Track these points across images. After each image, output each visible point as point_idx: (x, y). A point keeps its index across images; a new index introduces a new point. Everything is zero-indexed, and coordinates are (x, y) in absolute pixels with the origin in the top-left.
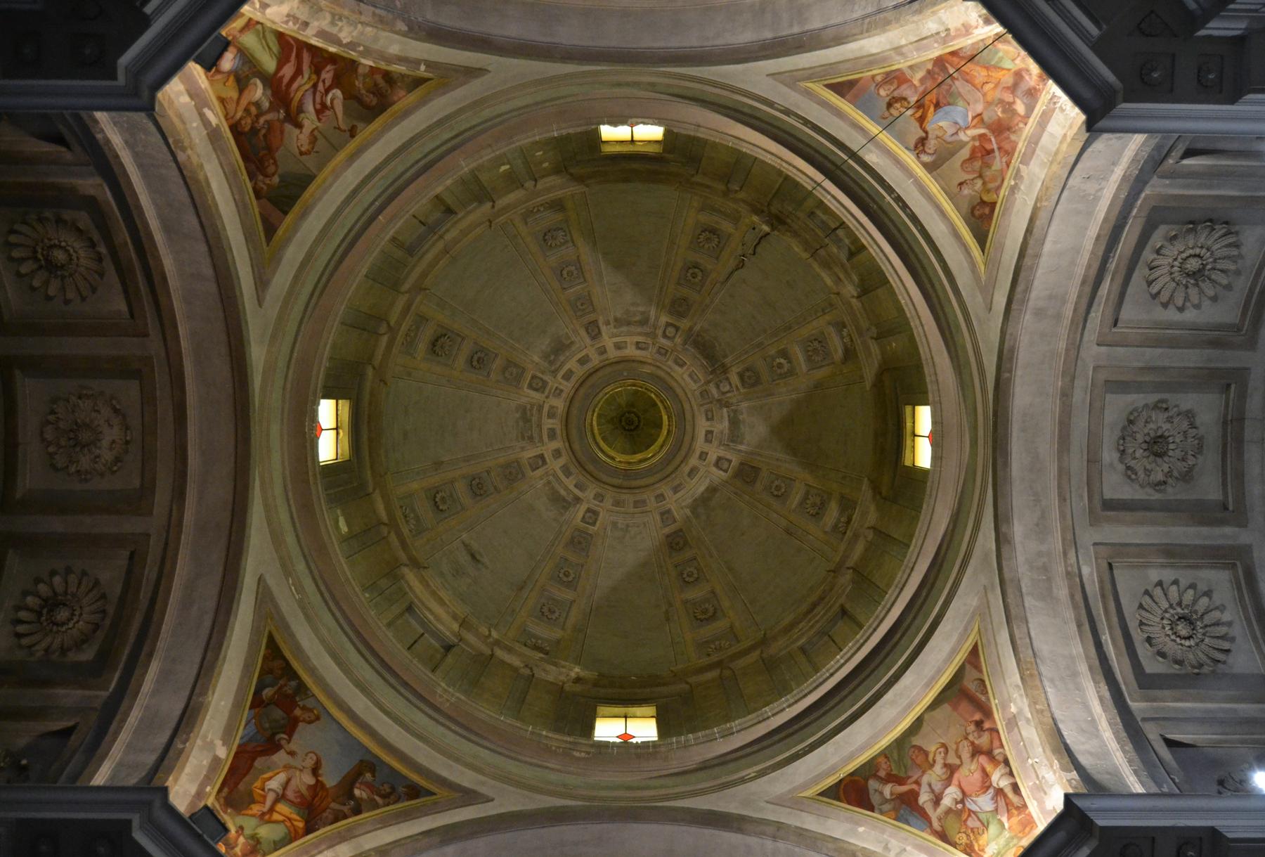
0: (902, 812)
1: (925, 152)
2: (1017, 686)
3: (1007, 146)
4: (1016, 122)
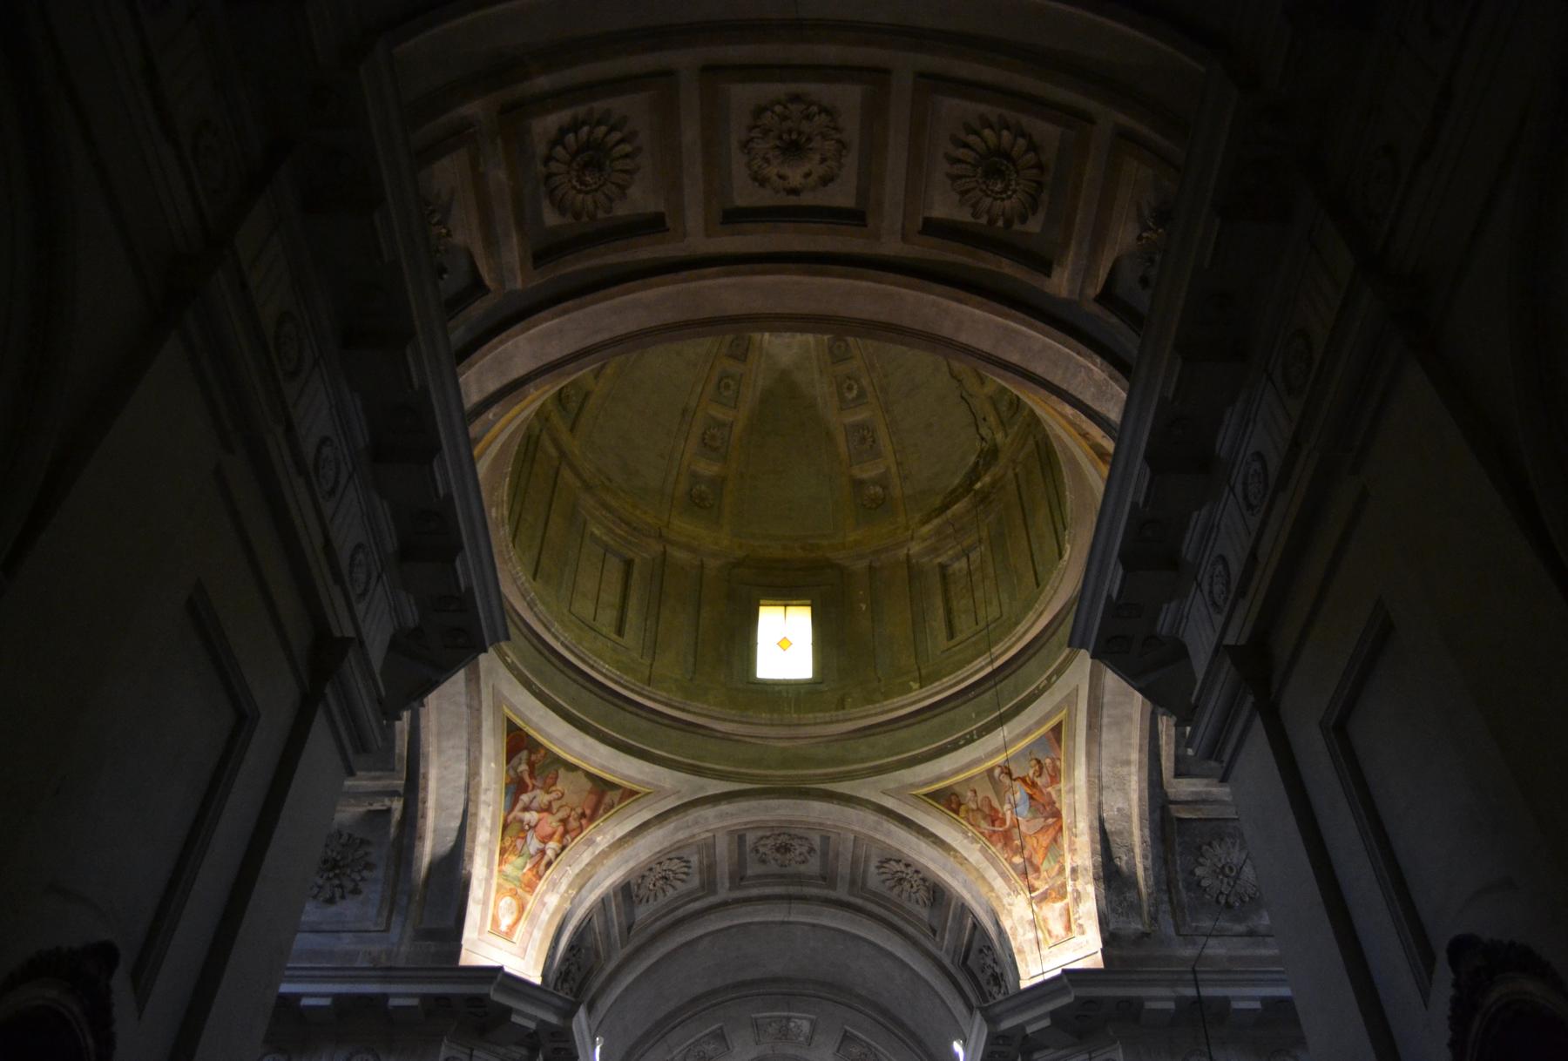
0: (512, 787)
2: (614, 836)
3: (995, 838)
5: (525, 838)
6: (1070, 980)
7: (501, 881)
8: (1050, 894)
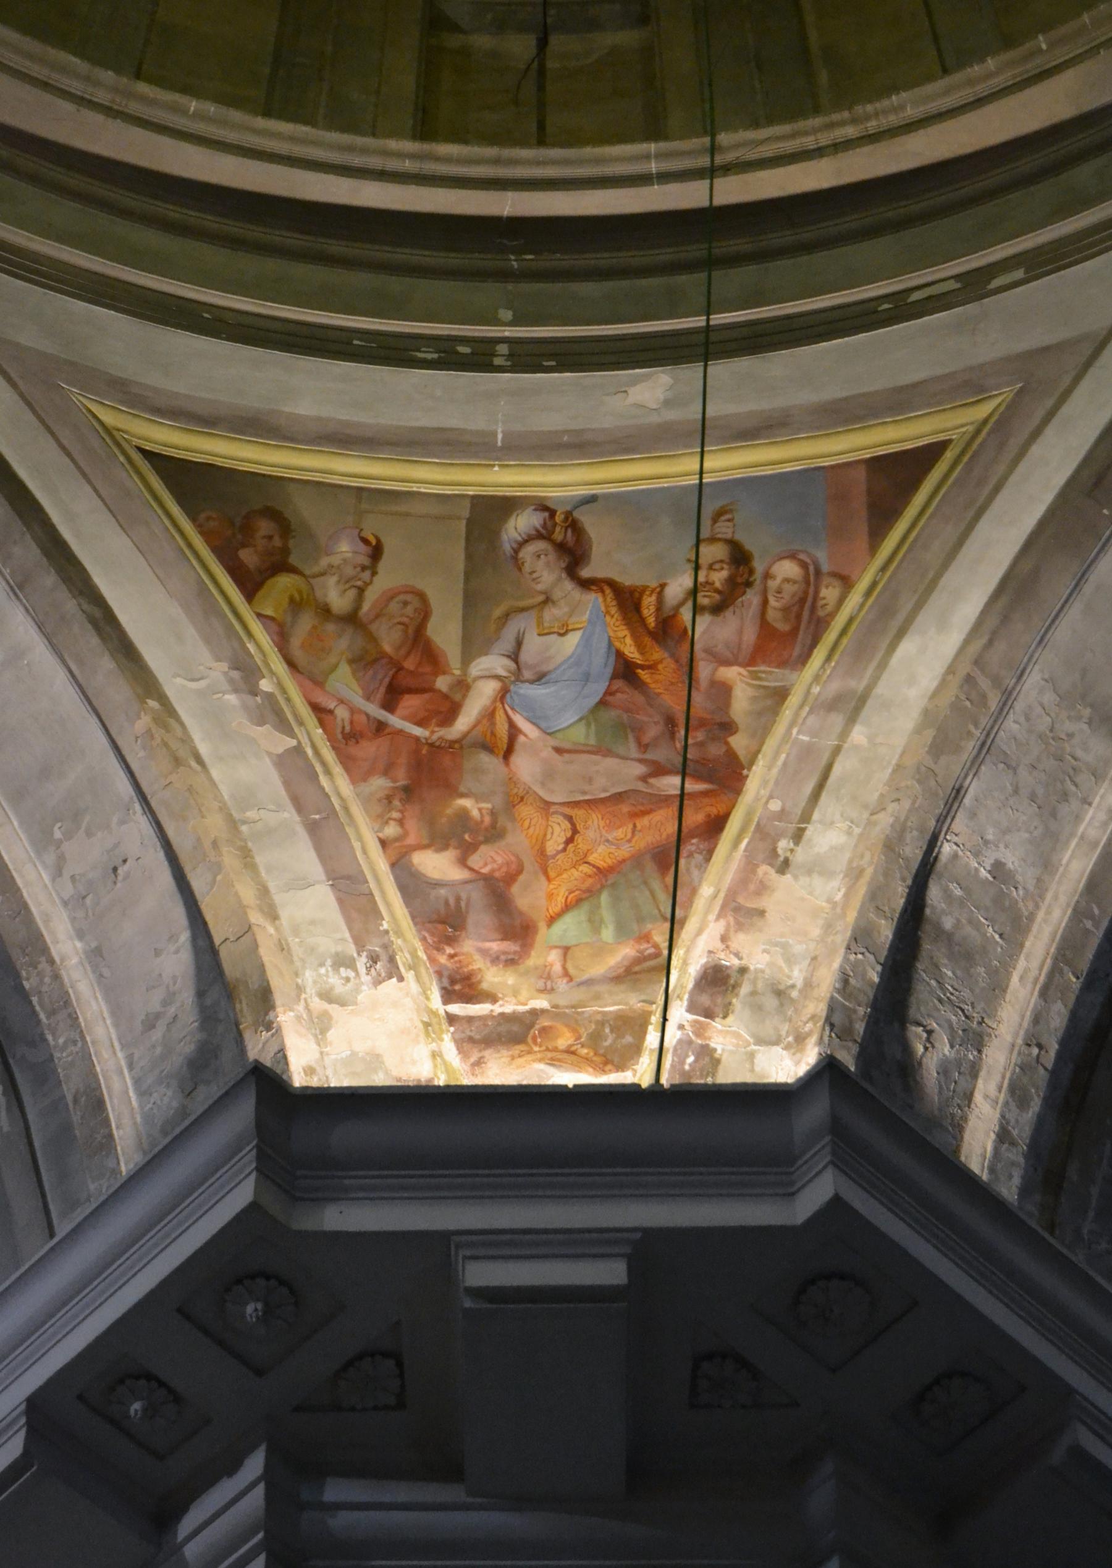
1: (539, 536)
3: (369, 749)
4: (412, 825)
6: (837, 1128)
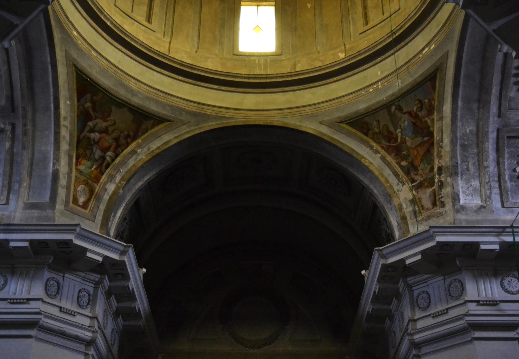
5: (92, 149)
7: (79, 175)
8: (424, 184)
